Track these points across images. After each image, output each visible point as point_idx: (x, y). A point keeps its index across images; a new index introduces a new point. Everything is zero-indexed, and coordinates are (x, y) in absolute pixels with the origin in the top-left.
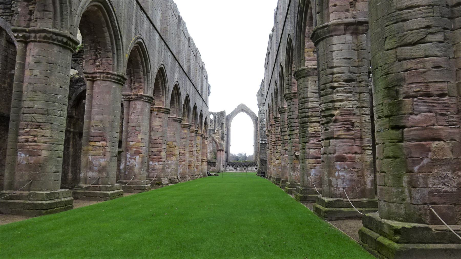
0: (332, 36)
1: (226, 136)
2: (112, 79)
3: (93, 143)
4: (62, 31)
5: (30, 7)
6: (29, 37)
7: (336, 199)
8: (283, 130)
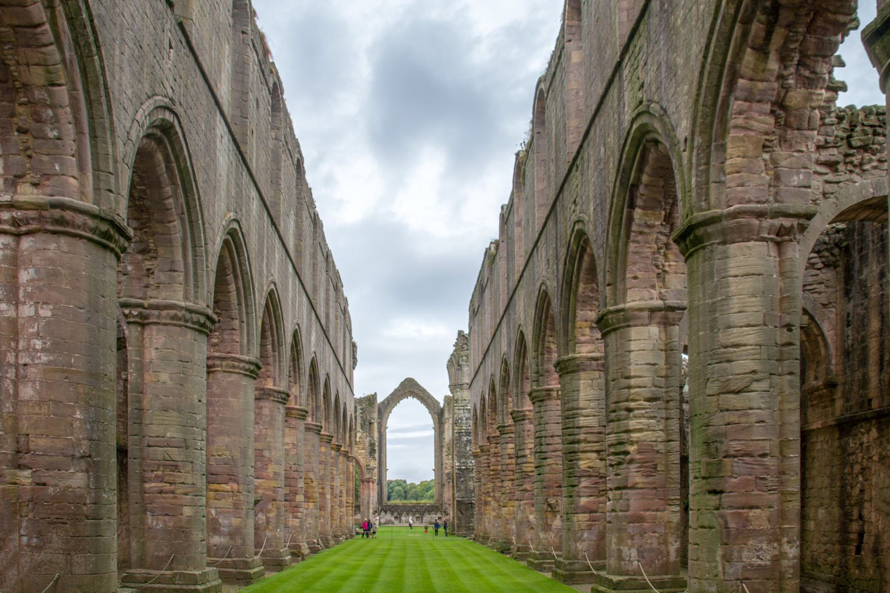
0: (629, 326)
1: (377, 449)
2: (241, 369)
4: (196, 303)
7: (627, 577)
8: (521, 453)
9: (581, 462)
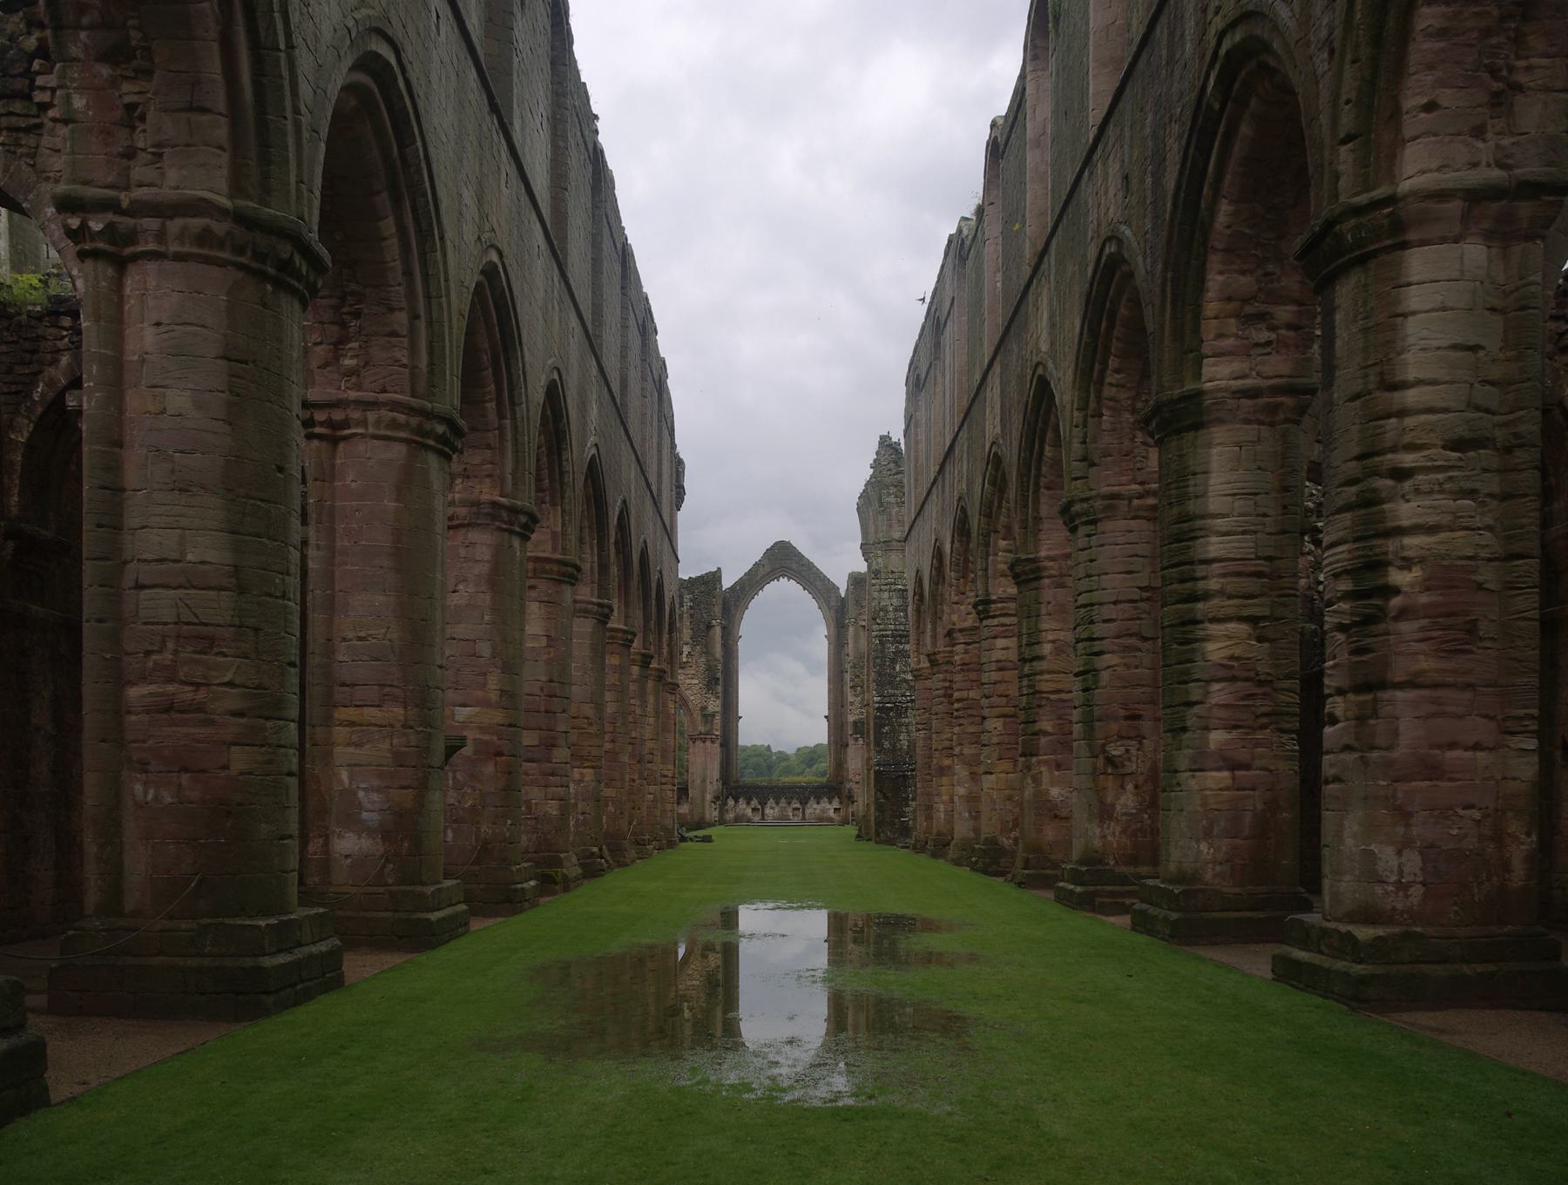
9: (1210, 646)
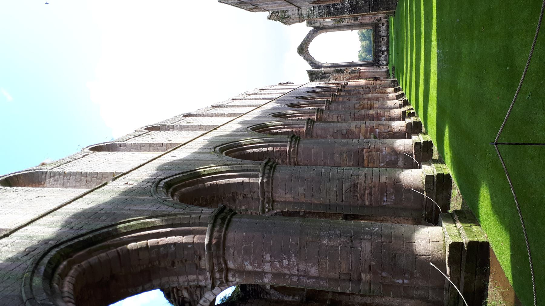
3: (366, 163)
5: (240, 198)
6: (269, 198)
